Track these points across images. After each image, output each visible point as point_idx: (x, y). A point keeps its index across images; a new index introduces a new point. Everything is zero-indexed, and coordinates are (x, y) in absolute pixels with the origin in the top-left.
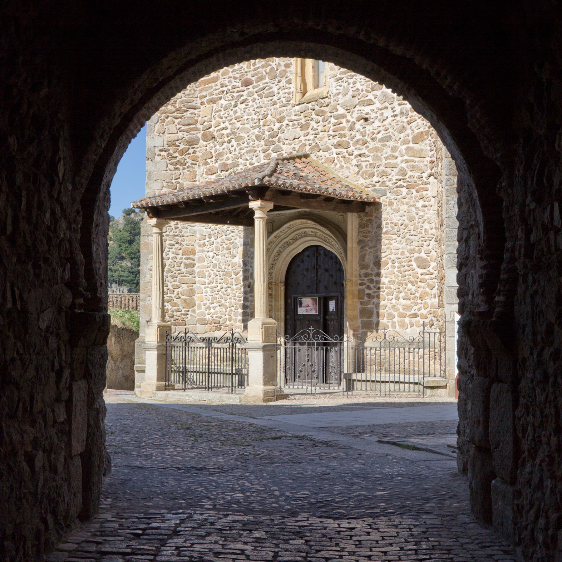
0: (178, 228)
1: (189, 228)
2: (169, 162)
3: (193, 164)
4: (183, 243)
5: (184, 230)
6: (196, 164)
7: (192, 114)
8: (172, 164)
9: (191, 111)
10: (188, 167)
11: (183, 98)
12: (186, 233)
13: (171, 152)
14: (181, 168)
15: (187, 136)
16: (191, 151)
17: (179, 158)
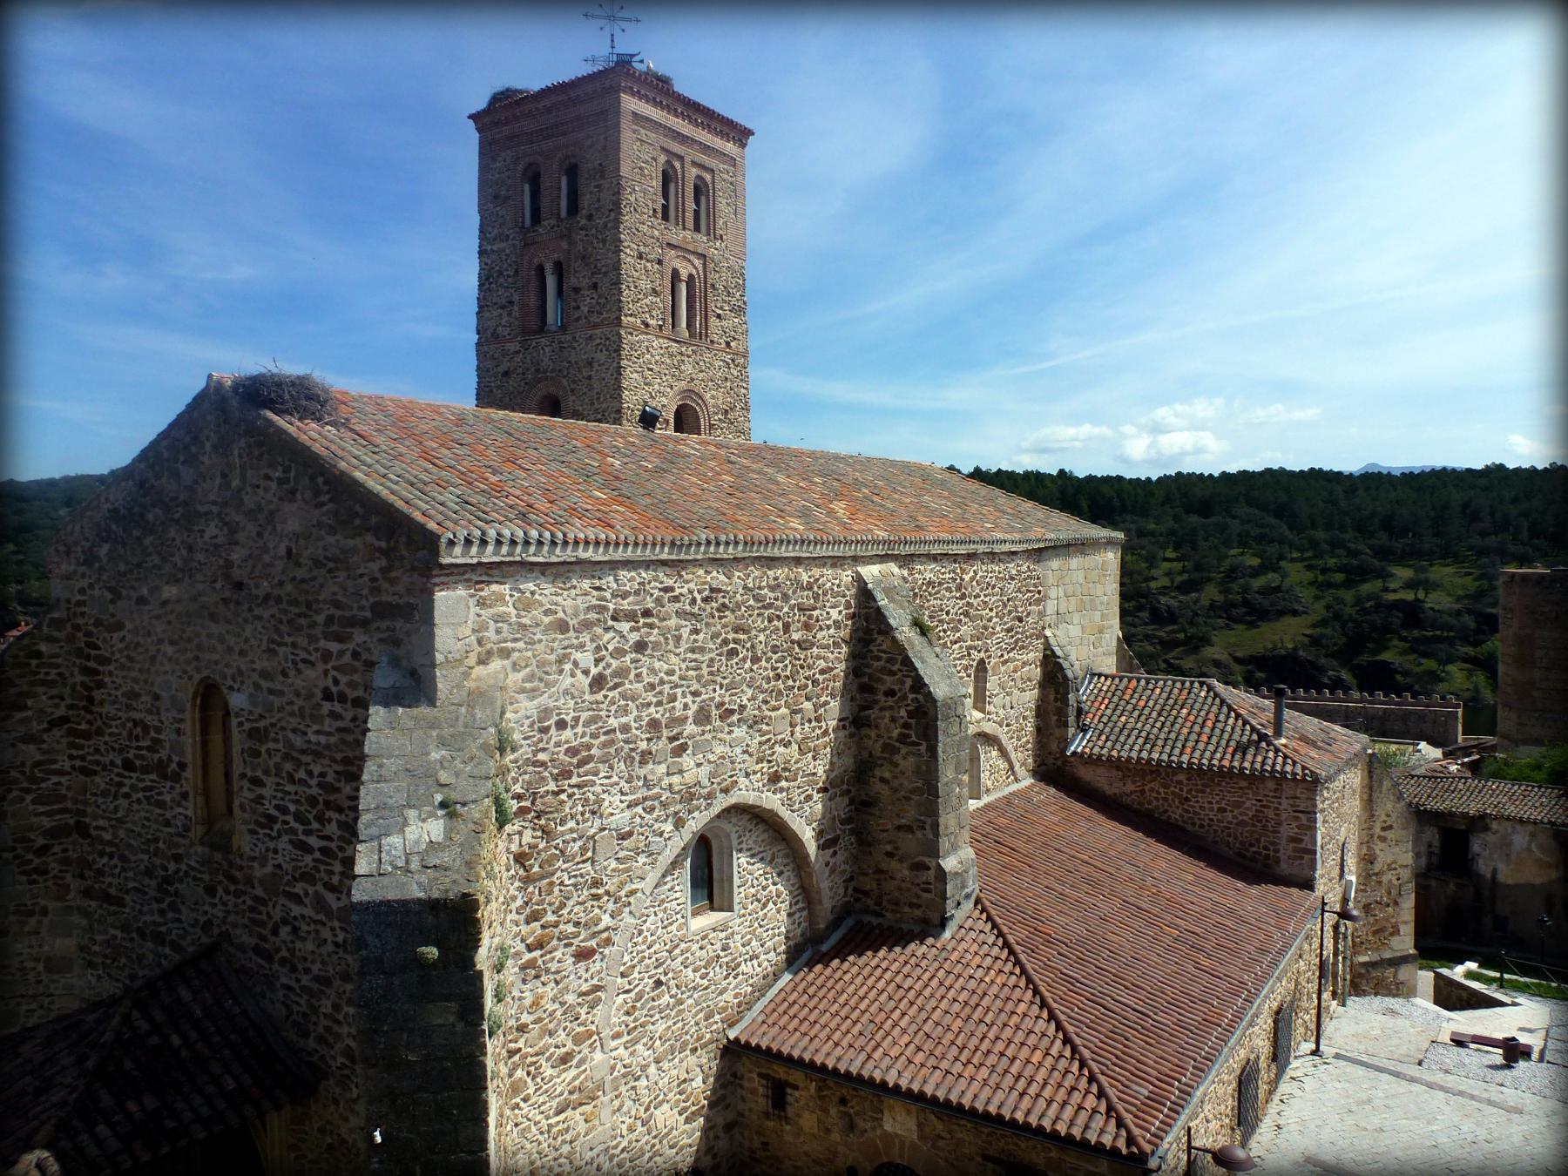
0: (40, 982)
1: (63, 980)
2: (17, 870)
3: (61, 871)
4: (52, 1007)
5: (52, 986)
6: (67, 871)
7: (55, 784)
8: (24, 873)
9: (55, 779)
10: (55, 877)
11: (39, 757)
12: (56, 988)
13: (20, 851)
14: (40, 879)
15: (47, 823)
16: (57, 849)
17: (37, 861)
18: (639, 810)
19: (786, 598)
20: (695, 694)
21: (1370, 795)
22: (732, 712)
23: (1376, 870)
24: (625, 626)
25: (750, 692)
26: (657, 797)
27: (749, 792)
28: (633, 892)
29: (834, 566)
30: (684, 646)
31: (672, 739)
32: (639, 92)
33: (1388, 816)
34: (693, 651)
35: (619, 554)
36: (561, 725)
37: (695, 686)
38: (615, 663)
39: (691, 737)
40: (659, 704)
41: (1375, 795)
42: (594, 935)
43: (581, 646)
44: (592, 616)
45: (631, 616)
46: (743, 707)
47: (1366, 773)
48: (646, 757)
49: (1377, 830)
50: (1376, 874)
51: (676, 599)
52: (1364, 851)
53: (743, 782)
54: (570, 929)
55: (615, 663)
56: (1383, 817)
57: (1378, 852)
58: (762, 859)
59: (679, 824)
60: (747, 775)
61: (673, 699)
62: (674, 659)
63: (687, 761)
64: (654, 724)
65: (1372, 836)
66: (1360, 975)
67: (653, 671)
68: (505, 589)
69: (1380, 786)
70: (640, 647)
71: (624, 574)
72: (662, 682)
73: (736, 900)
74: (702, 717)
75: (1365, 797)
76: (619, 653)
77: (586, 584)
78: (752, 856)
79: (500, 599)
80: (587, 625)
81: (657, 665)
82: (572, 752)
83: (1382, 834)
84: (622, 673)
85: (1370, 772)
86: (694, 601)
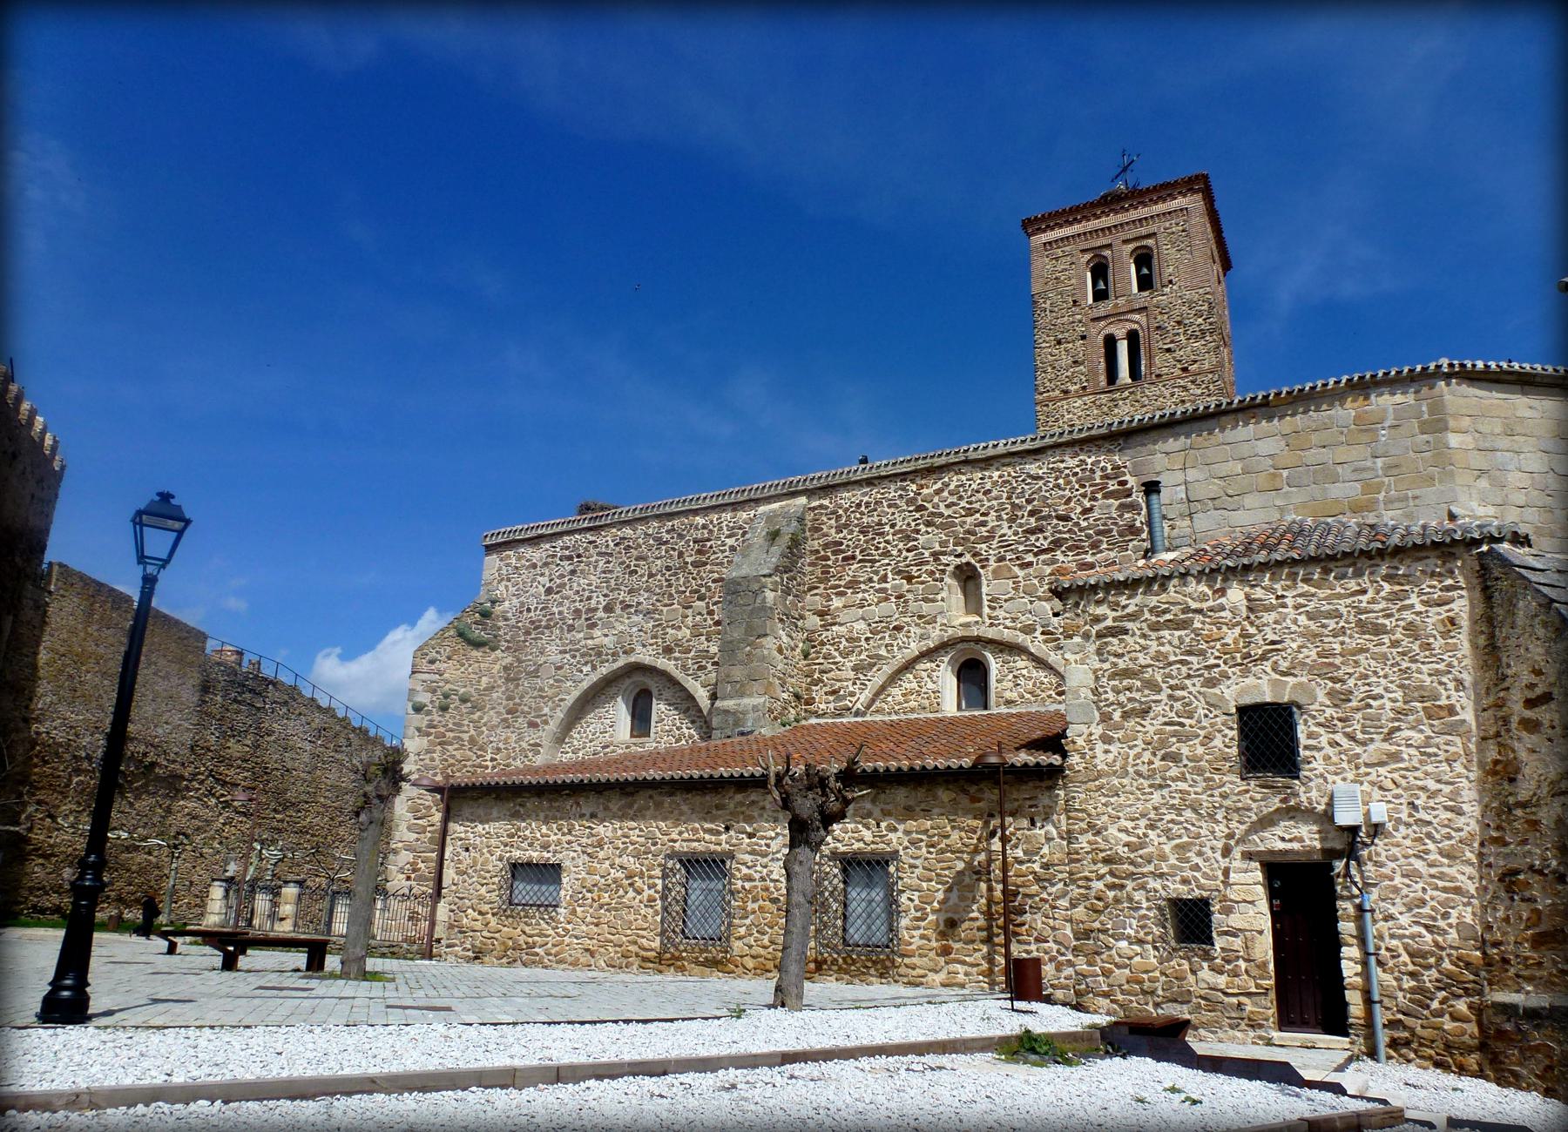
18: (568, 656)
19: (681, 536)
20: (605, 596)
21: (1492, 636)
22: (631, 606)
23: (1523, 795)
24: (566, 563)
25: (646, 595)
26: (578, 650)
27: (644, 656)
28: (561, 700)
29: (734, 510)
30: (599, 569)
31: (587, 619)
32: (1103, 212)
33: (1538, 673)
34: (604, 572)
35: (559, 529)
36: (529, 610)
37: (605, 591)
38: (558, 581)
39: (600, 619)
40: (581, 601)
41: (1501, 634)
42: (538, 716)
43: (542, 575)
44: (550, 560)
45: (570, 558)
46: (639, 604)
47: (1477, 594)
48: (571, 628)
49: (1517, 709)
50: (1523, 805)
51: (596, 547)
52: (1492, 754)
53: (639, 648)
54: (526, 709)
55: (558, 581)
56: (1527, 677)
57: (1523, 755)
58: (676, 709)
59: (594, 668)
60: (644, 646)
61: (589, 598)
62: (592, 577)
63: (597, 632)
64: (577, 611)
65: (1506, 721)
66: (1501, 1034)
67: (579, 585)
68: (511, 553)
69: (1511, 605)
70: (573, 572)
71: (566, 538)
72: (584, 590)
73: (653, 730)
74: (609, 609)
75: (1482, 640)
76: (562, 576)
77: (548, 546)
78: (669, 705)
79: (509, 557)
80: (546, 564)
81: (582, 581)
82: (532, 622)
83: (1528, 714)
84: (563, 585)
85: (1485, 589)
86: (607, 546)
